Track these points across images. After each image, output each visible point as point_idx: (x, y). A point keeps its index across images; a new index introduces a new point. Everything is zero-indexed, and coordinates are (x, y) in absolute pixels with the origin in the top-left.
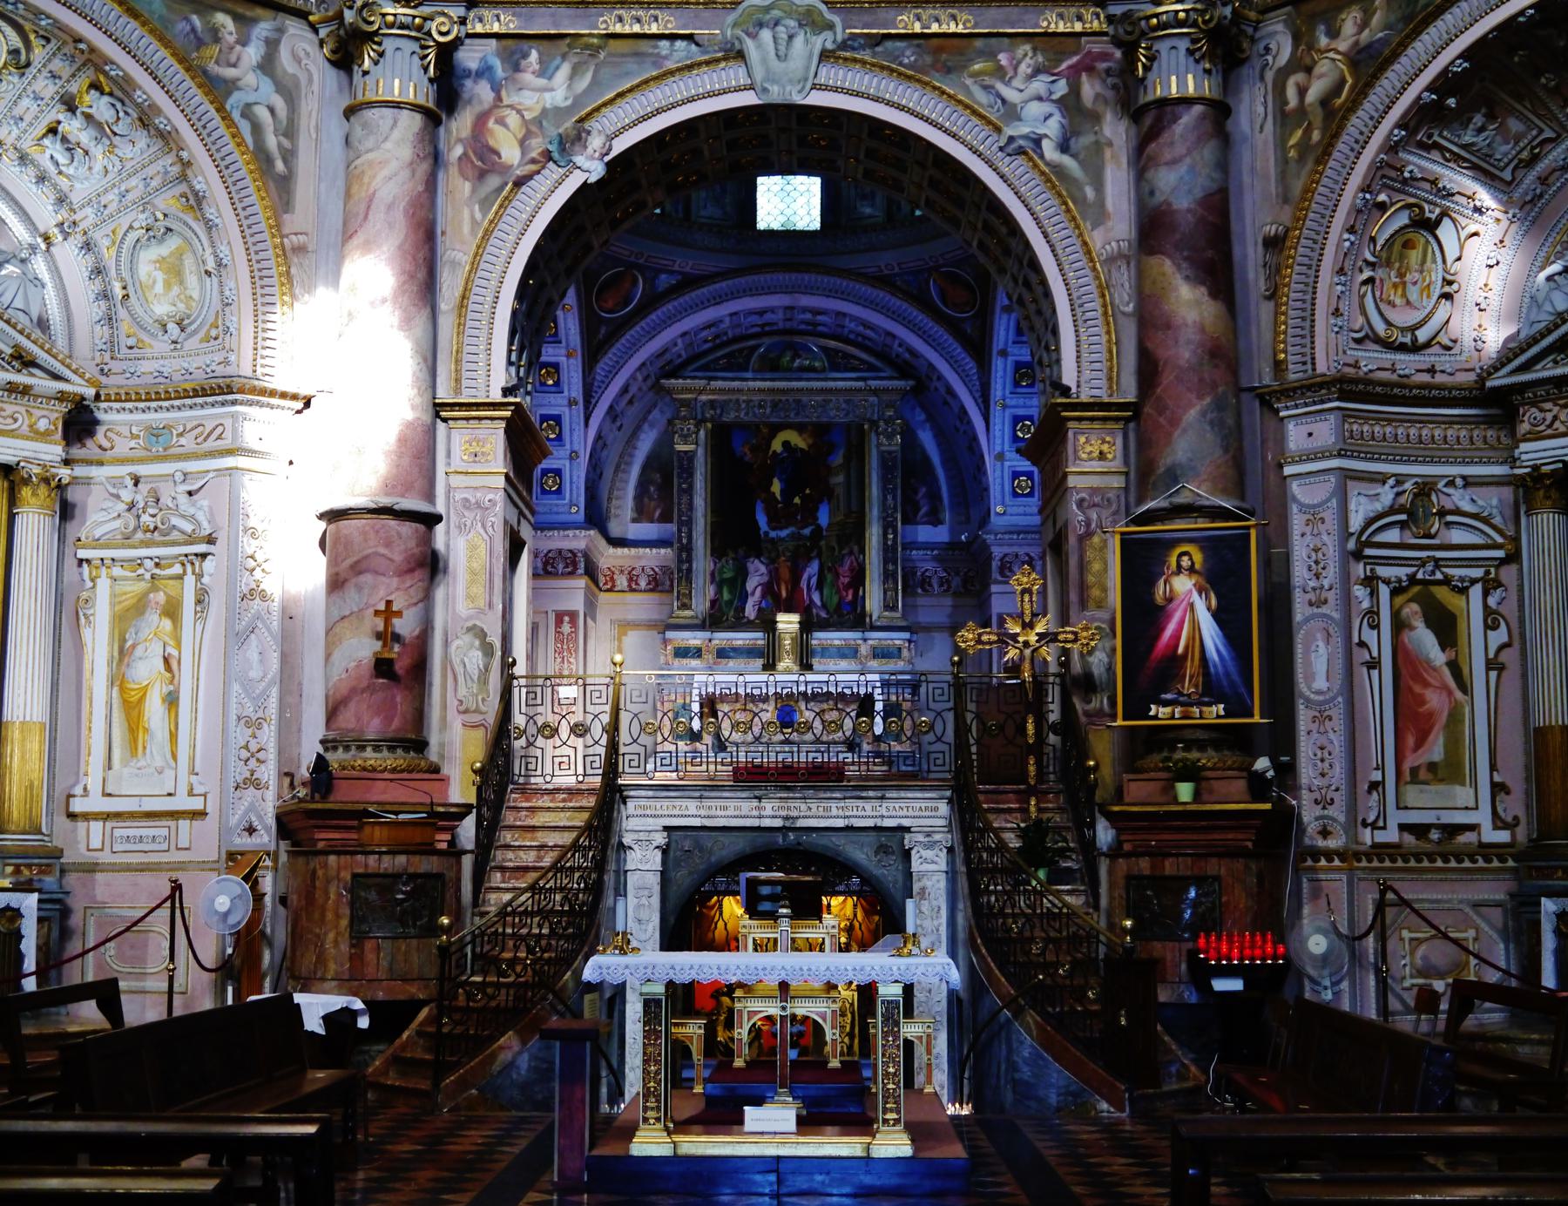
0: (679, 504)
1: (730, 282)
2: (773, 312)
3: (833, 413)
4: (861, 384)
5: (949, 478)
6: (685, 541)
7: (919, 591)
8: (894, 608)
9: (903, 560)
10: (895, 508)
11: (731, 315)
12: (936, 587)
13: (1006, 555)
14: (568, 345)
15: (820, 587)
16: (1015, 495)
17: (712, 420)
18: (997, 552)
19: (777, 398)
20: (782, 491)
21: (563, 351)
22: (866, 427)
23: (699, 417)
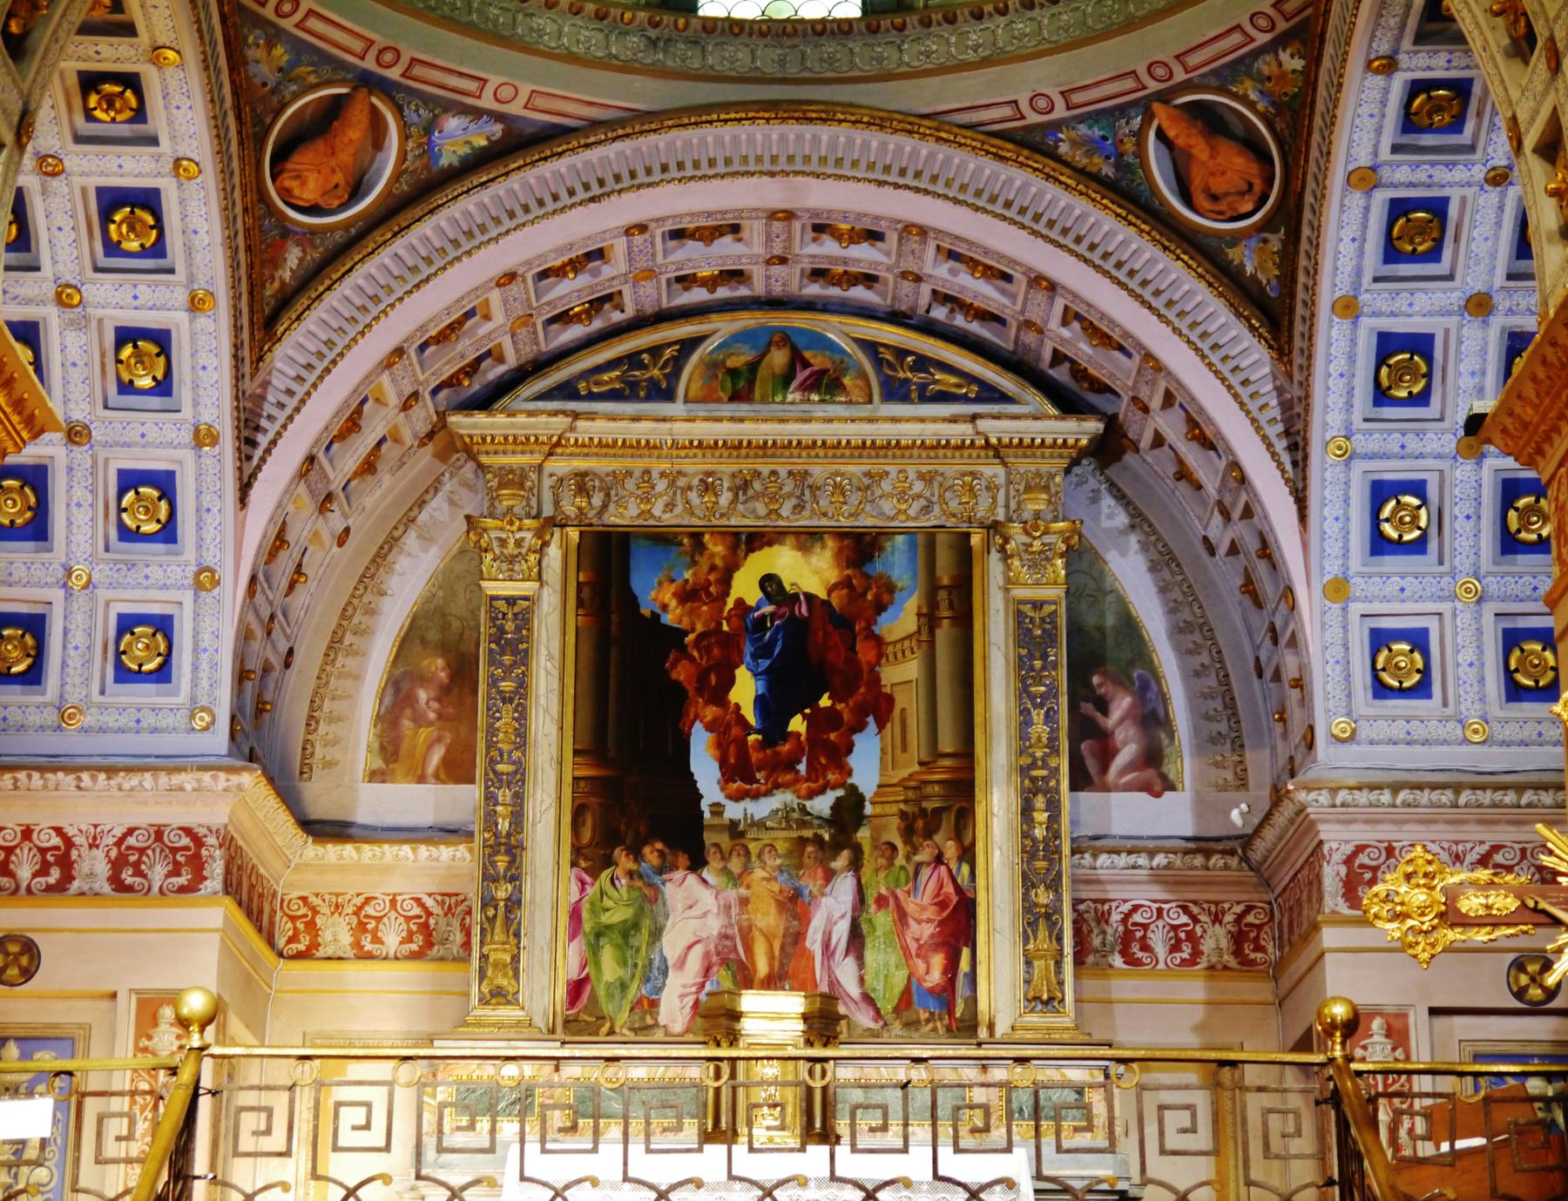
0: (491, 731)
1: (625, 146)
2: (735, 229)
3: (888, 506)
4: (965, 429)
5: (1193, 675)
6: (504, 825)
7: (1118, 961)
8: (1051, 1003)
9: (1075, 881)
10: (1054, 749)
11: (628, 232)
12: (1161, 950)
13: (1360, 849)
14: (191, 278)
15: (856, 940)
16: (1381, 690)
17: (581, 520)
18: (1337, 839)
19: (746, 466)
20: (760, 701)
21: (181, 296)
22: (976, 540)
23: (548, 511)
